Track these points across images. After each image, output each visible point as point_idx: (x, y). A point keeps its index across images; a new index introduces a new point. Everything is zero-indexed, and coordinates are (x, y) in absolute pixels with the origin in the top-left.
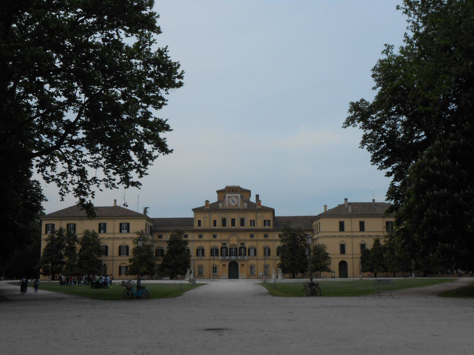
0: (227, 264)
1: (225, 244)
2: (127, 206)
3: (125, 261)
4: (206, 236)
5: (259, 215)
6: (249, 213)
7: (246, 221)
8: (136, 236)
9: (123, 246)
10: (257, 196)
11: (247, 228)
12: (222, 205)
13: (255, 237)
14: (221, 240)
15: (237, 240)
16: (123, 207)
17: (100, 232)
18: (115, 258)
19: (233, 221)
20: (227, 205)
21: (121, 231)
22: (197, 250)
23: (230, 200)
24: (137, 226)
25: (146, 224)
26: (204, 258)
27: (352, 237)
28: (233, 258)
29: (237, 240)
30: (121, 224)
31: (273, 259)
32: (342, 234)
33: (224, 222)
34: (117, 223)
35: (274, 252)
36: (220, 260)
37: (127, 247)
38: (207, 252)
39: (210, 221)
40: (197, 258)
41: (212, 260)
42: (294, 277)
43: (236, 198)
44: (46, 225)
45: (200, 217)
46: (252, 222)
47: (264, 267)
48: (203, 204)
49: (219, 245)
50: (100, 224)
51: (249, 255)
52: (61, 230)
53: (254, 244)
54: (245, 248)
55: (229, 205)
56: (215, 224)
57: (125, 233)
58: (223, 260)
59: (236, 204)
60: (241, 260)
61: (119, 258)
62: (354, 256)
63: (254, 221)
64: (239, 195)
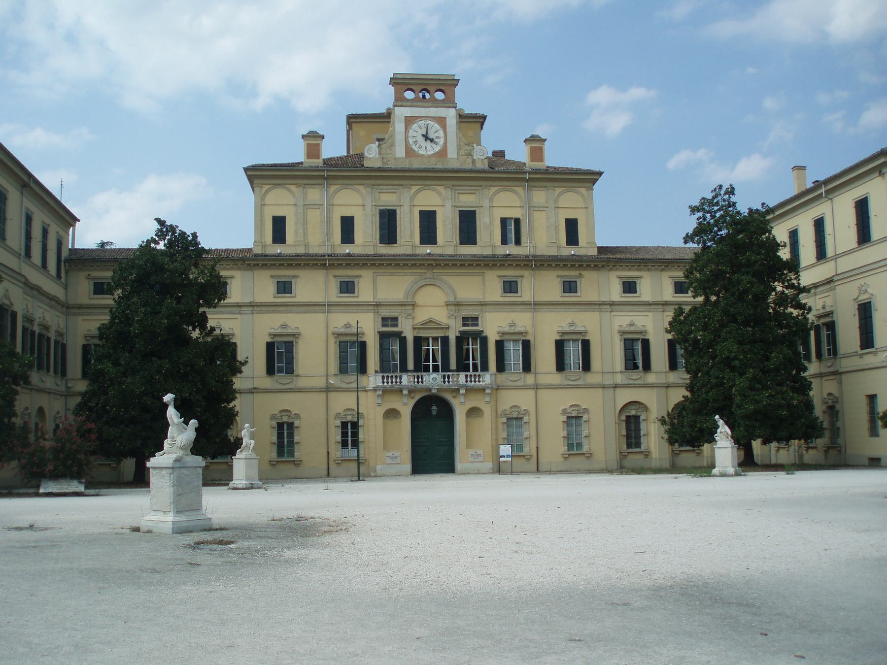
0: (406, 410)
4: (311, 286)
6: (494, 189)
7: (482, 221)
12: (380, 153)
13: (526, 293)
14: (378, 305)
15: (447, 305)
22: (270, 346)
23: (411, 131)
28: (432, 380)
29: (447, 305)
31: (603, 387)
36: (375, 389)
38: (315, 357)
39: (329, 220)
40: (266, 382)
41: (338, 390)
43: (437, 126)
45: (283, 201)
46: (512, 227)
47: (564, 418)
51: (501, 367)
55: (409, 152)
58: (385, 391)
59: (437, 148)
60: (469, 390)
63: (517, 221)
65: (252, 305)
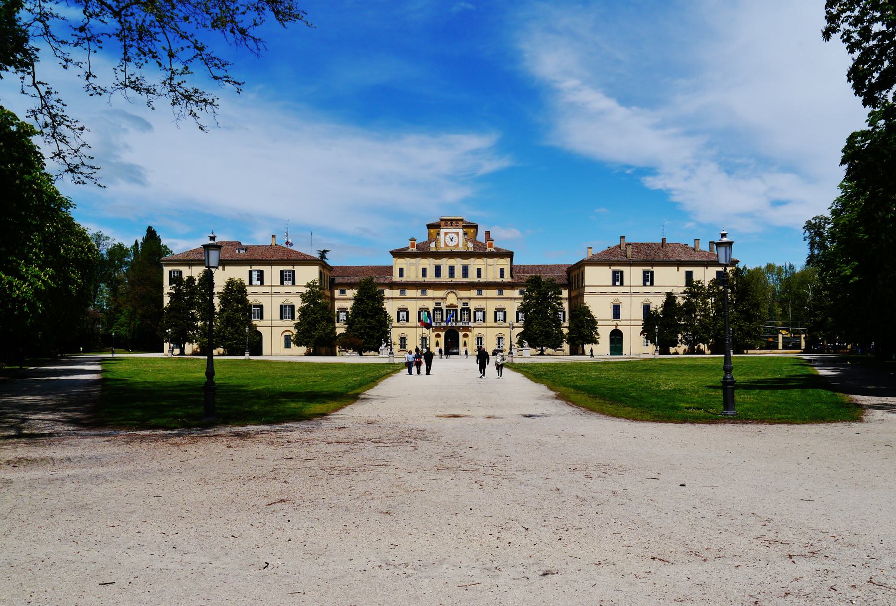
0: (443, 334)
1: (439, 304)
2: (291, 245)
3: (290, 326)
4: (410, 293)
5: (490, 261)
8: (304, 290)
9: (286, 306)
10: (487, 233)
11: (472, 280)
14: (434, 299)
16: (285, 245)
17: (251, 283)
18: (274, 323)
19: (452, 269)
20: (442, 245)
21: (282, 283)
24: (308, 275)
25: (321, 273)
26: (408, 324)
27: (631, 294)
30: (282, 272)
32: (615, 289)
33: (438, 270)
34: (277, 269)
35: (511, 317)
37: (293, 307)
42: (542, 354)
44: (170, 272)
48: (409, 244)
49: (431, 306)
50: (251, 272)
52: (191, 279)
53: (482, 304)
54: (468, 310)
55: (446, 245)
56: (424, 275)
57: (288, 285)
61: (281, 323)
62: (633, 323)
64: (461, 231)
65: (392, 299)
